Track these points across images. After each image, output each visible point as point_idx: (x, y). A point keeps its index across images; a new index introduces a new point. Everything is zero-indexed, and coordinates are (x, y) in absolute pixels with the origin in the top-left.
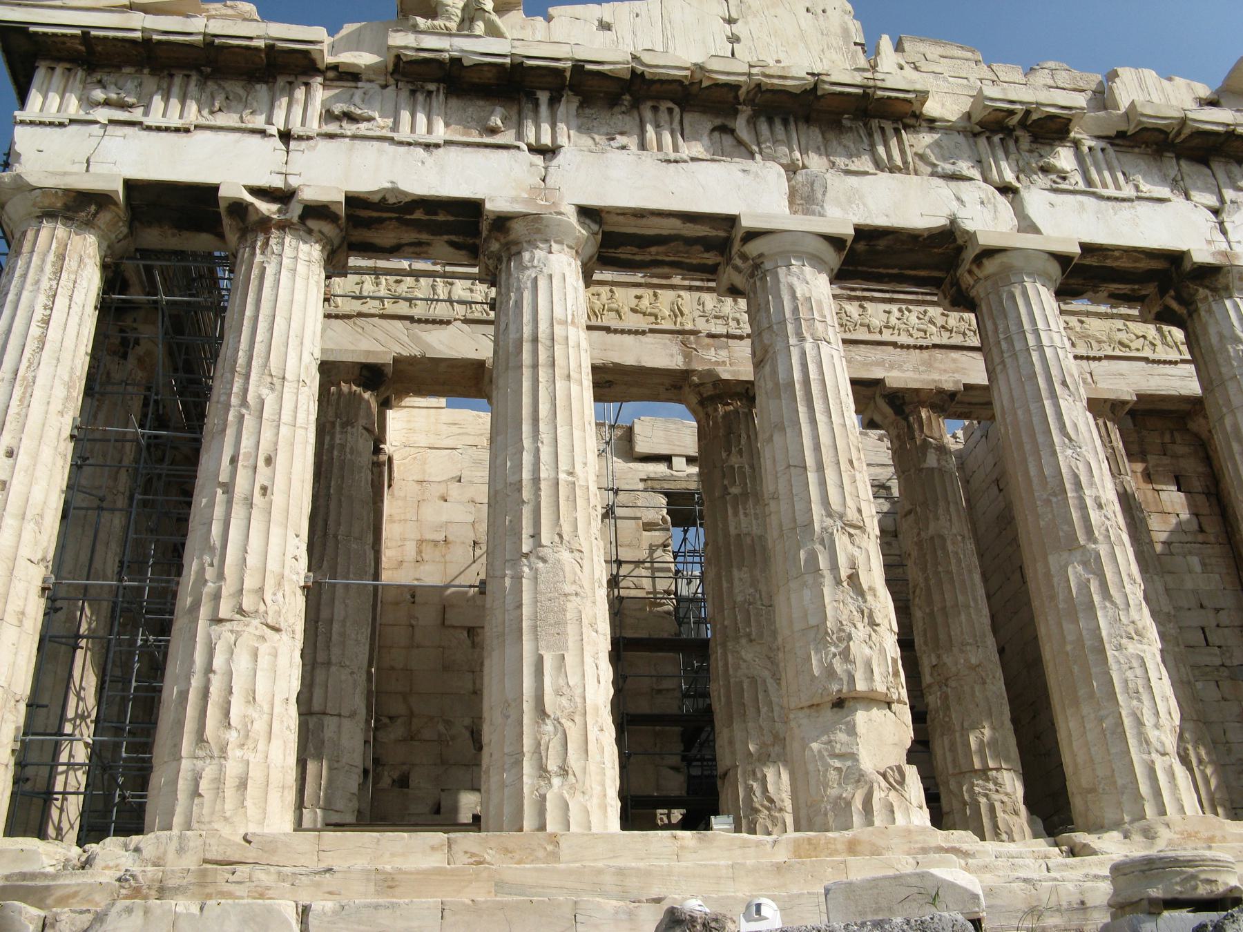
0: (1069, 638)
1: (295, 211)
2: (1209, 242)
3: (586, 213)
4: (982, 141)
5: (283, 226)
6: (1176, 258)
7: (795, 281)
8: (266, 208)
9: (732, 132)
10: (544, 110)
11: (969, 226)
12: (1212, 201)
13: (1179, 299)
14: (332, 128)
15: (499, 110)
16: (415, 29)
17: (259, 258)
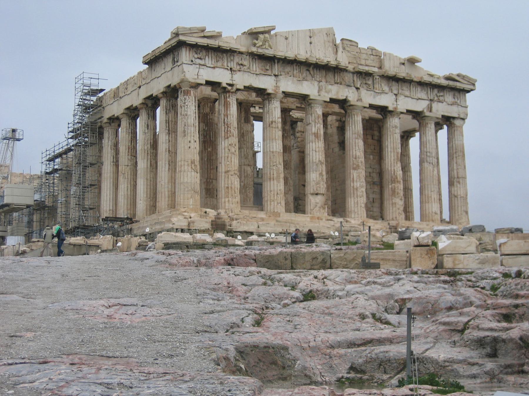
0: (352, 185)
1: (234, 89)
2: (393, 104)
3: (283, 92)
4: (355, 75)
5: (232, 92)
6: (386, 107)
7: (317, 110)
8: (229, 88)
9: (309, 71)
10: (276, 64)
11: (349, 99)
12: (396, 92)
13: (384, 114)
14: (238, 67)
15: (268, 65)
16: (255, 45)
17: (228, 100)
